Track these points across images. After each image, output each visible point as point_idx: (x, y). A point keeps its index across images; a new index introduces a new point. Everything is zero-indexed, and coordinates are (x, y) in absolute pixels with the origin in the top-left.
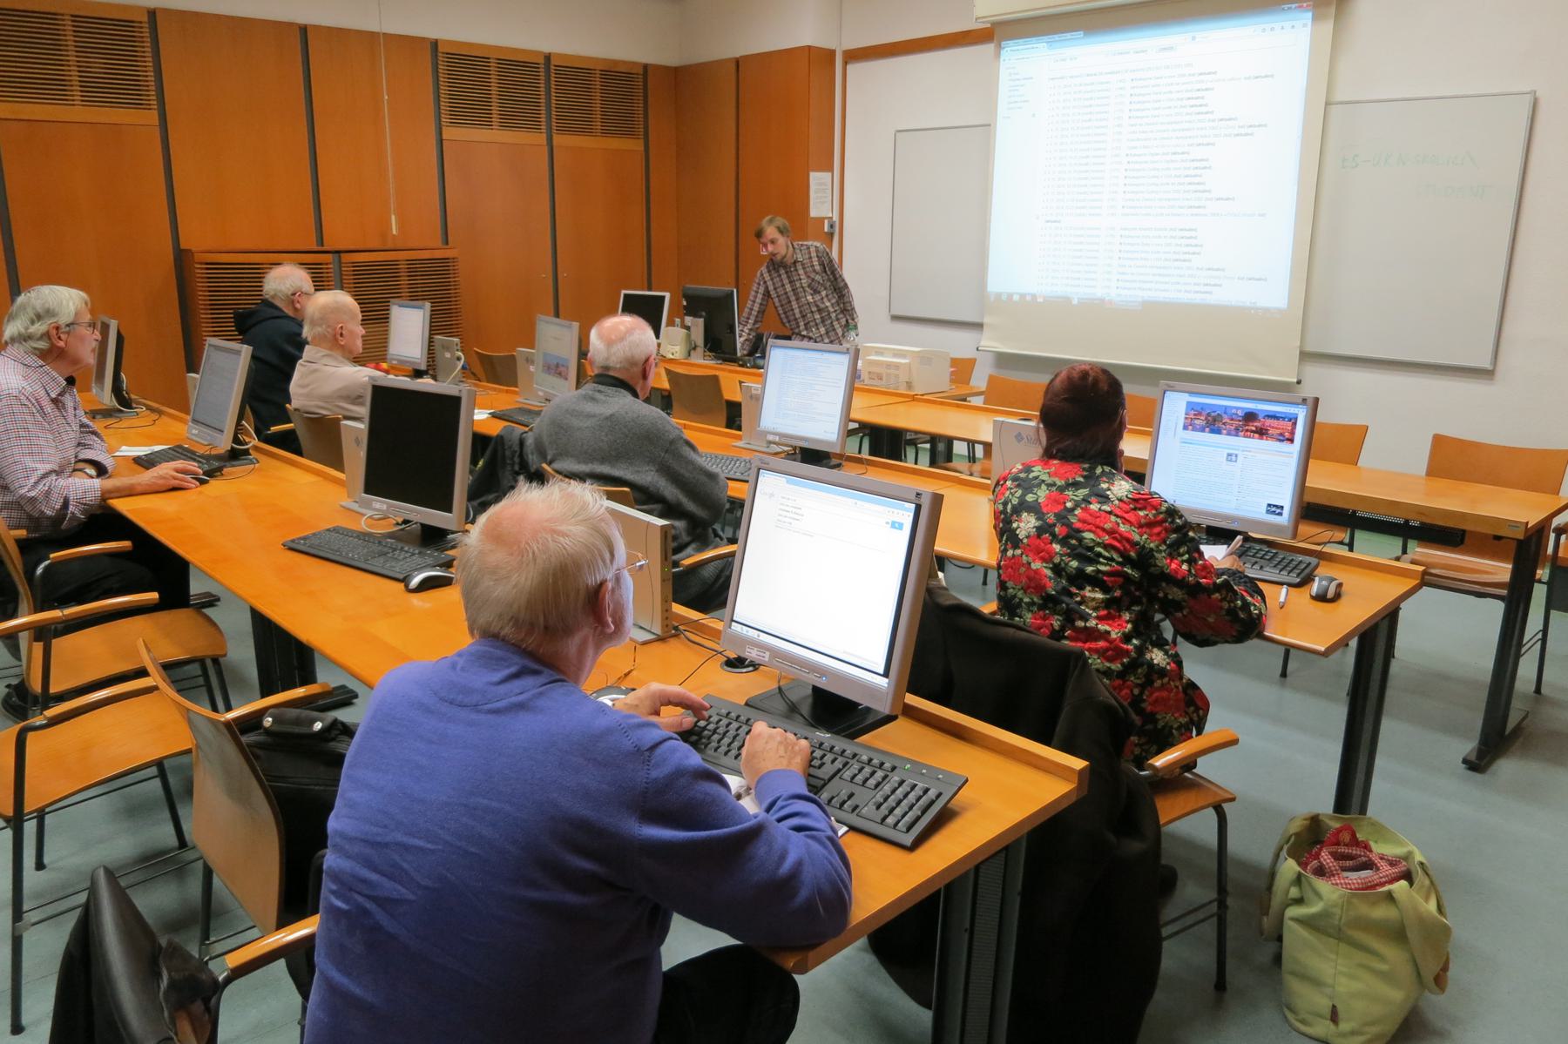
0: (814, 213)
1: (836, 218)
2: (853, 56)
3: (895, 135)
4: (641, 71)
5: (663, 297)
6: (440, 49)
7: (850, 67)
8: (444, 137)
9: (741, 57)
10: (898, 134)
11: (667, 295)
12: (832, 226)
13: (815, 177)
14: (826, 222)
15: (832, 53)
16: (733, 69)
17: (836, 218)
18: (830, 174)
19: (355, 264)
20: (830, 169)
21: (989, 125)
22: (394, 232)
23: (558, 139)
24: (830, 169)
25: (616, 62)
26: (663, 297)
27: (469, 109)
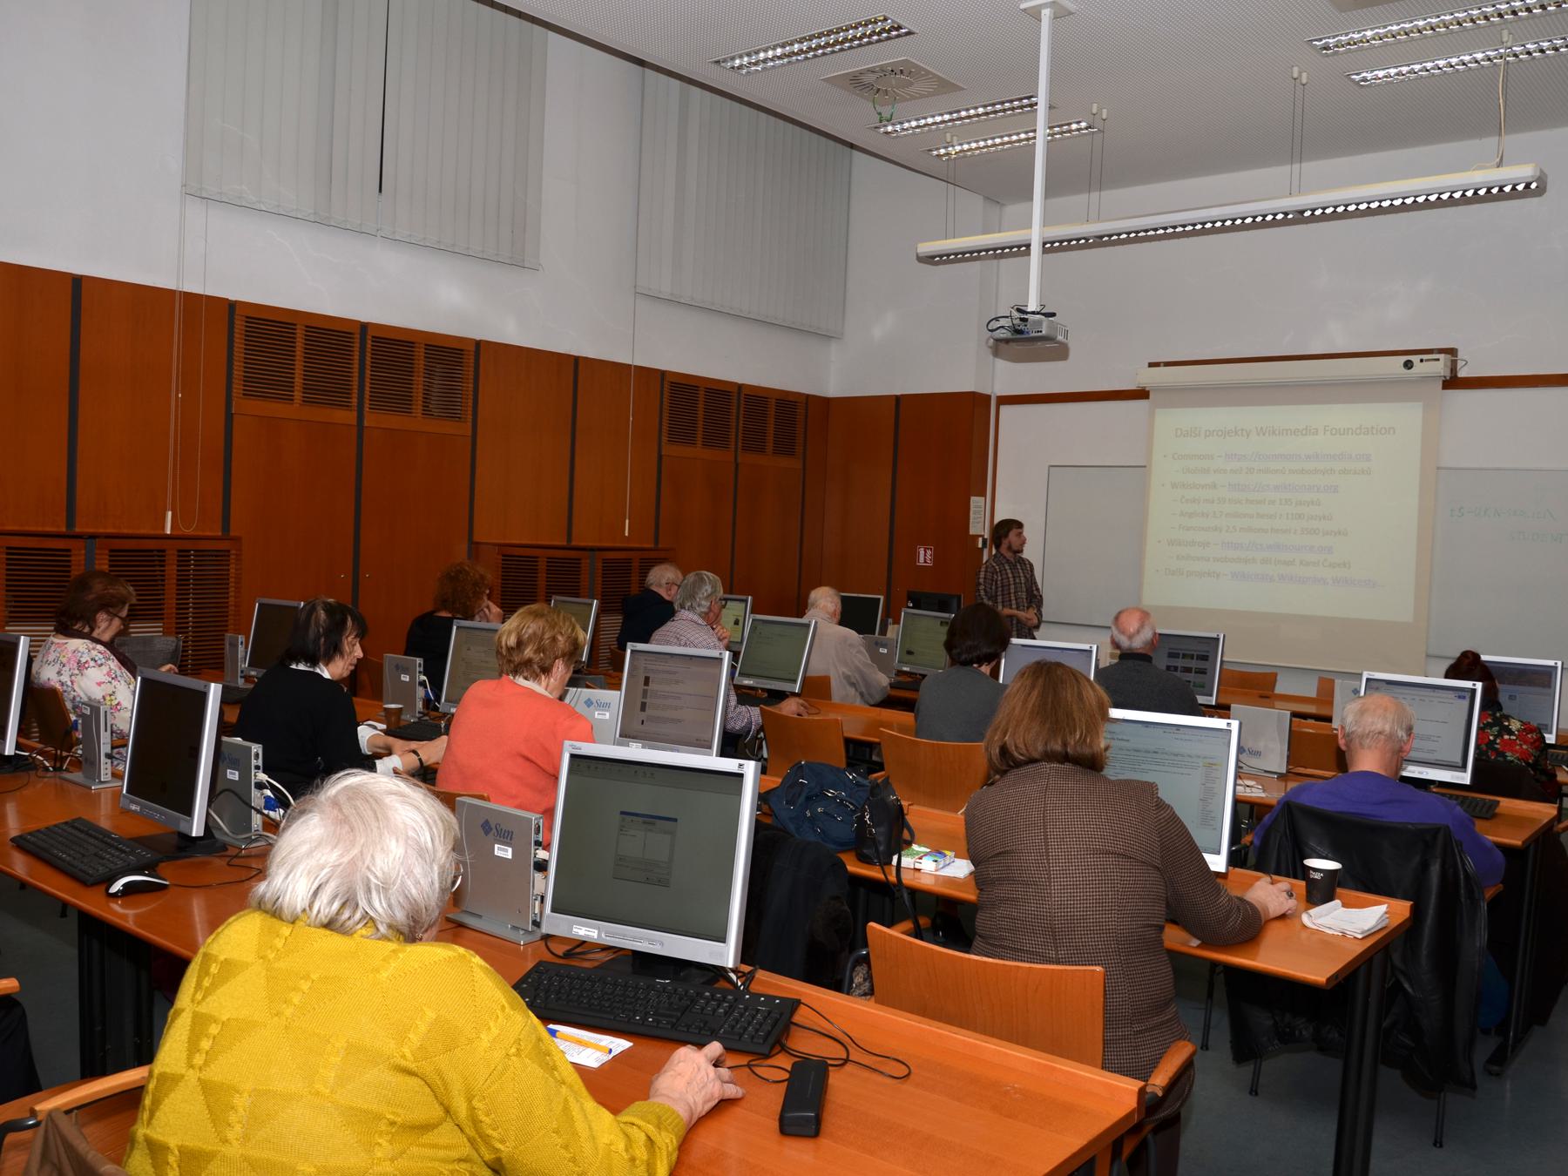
0: (972, 532)
3: (1049, 471)
5: (879, 599)
7: (1004, 409)
9: (902, 395)
10: (1052, 469)
11: (882, 598)
13: (973, 499)
15: (989, 397)
16: (894, 403)
18: (983, 498)
19: (605, 561)
20: (983, 494)
21: (1145, 467)
22: (627, 534)
24: (983, 494)
26: (879, 599)
27: (681, 431)
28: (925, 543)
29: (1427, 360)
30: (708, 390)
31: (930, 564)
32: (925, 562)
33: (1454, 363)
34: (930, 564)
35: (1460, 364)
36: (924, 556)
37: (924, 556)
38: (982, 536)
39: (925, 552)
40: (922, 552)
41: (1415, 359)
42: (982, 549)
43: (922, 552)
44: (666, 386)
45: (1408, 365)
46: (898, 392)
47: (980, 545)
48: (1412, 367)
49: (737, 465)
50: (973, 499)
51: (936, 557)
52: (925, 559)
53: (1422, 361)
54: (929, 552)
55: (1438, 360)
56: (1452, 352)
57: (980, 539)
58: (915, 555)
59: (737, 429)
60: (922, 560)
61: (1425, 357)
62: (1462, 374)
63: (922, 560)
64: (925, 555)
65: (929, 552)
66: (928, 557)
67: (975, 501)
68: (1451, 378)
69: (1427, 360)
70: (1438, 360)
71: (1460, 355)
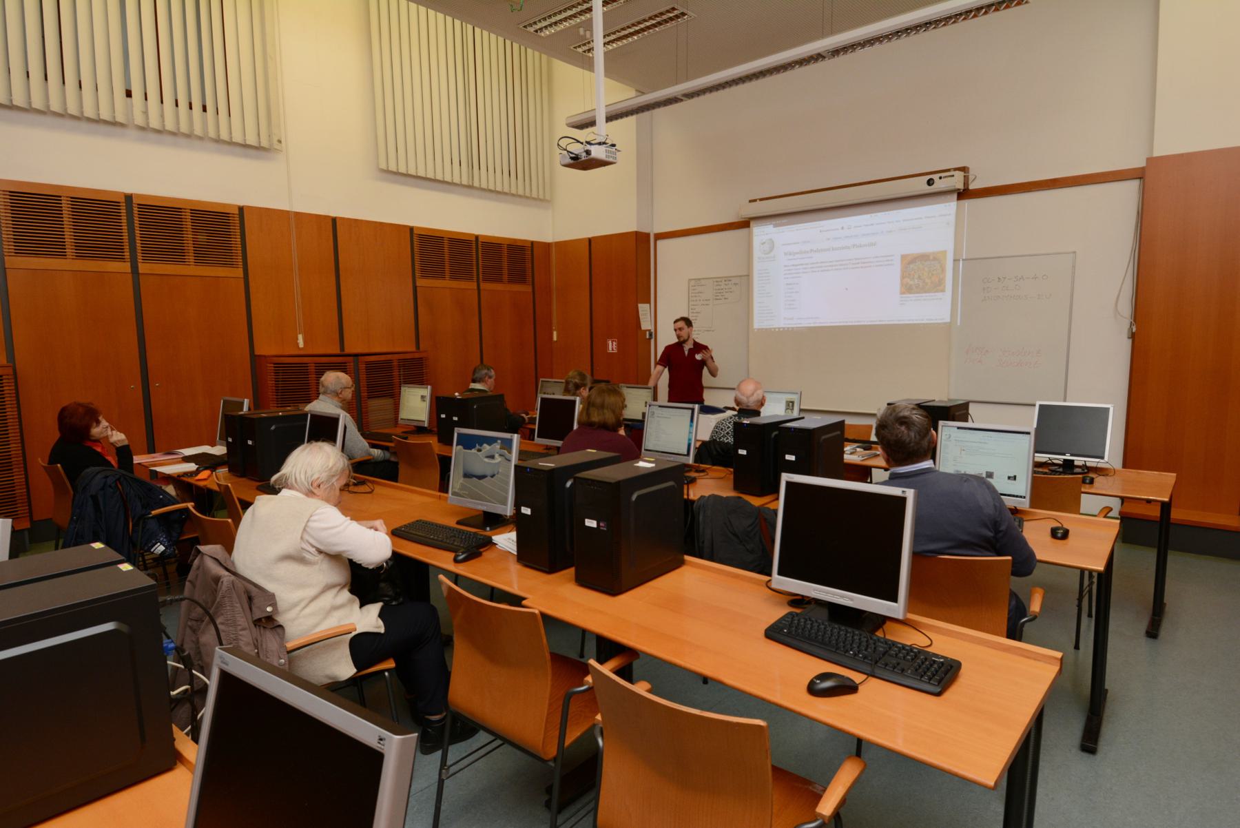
0: (643, 327)
1: (653, 331)
2: (661, 236)
4: (474, 239)
6: (415, 232)
7: (660, 243)
8: (418, 285)
12: (651, 335)
13: (640, 306)
14: (648, 333)
15: (648, 235)
17: (653, 331)
18: (648, 305)
20: (648, 302)
23: (484, 286)
24: (648, 302)
28: (611, 337)
29: (946, 177)
30: (451, 240)
31: (615, 351)
32: (613, 350)
33: (966, 179)
35: (971, 178)
36: (612, 346)
37: (612, 346)
38: (649, 330)
40: (610, 343)
41: (935, 177)
42: (650, 339)
43: (610, 343)
44: (415, 239)
45: (930, 182)
47: (648, 337)
48: (933, 184)
50: (640, 306)
53: (940, 178)
54: (614, 343)
55: (953, 176)
56: (964, 169)
57: (648, 333)
58: (606, 346)
59: (478, 268)
60: (610, 349)
61: (943, 175)
62: (971, 187)
63: (610, 349)
65: (614, 343)
66: (614, 346)
67: (643, 308)
68: (964, 190)
69: (946, 177)
70: (953, 176)
71: (971, 172)
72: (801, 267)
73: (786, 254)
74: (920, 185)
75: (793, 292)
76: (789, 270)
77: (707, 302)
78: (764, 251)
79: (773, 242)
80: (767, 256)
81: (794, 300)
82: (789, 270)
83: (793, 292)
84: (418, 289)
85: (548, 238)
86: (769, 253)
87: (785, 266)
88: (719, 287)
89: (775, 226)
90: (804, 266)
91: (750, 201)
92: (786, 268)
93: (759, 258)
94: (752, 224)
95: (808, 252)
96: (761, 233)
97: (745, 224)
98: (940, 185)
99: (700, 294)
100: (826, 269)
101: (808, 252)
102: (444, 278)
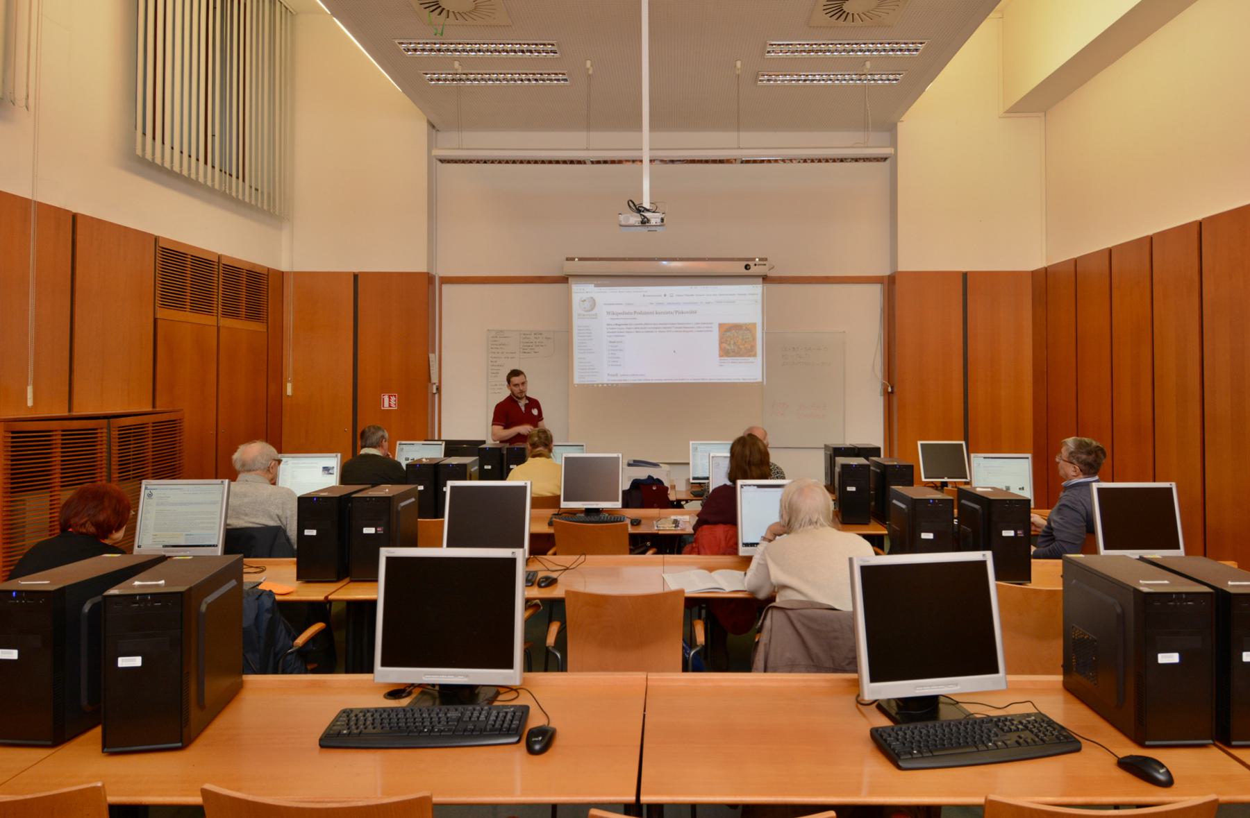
9: (361, 273)
24: (434, 352)
25: (254, 265)
28: (387, 389)
31: (394, 408)
32: (390, 406)
34: (394, 408)
39: (390, 398)
40: (386, 399)
43: (386, 399)
46: (356, 270)
49: (218, 328)
51: (400, 403)
52: (390, 404)
54: (393, 399)
58: (381, 402)
60: (386, 404)
63: (386, 404)
64: (390, 401)
65: (393, 399)
72: (624, 327)
73: (608, 313)
74: (739, 268)
75: (616, 350)
76: (613, 329)
77: (514, 355)
78: (585, 308)
79: (594, 300)
80: (588, 313)
81: (618, 358)
82: (613, 329)
83: (616, 350)
84: (159, 322)
85: (284, 267)
86: (592, 309)
87: (608, 325)
88: (527, 340)
89: (597, 286)
90: (628, 326)
91: (568, 259)
92: (608, 327)
93: (579, 315)
94: (570, 279)
95: (631, 313)
96: (581, 292)
97: (564, 279)
98: (753, 270)
99: (502, 346)
100: (650, 330)
101: (631, 313)
102: (182, 308)
